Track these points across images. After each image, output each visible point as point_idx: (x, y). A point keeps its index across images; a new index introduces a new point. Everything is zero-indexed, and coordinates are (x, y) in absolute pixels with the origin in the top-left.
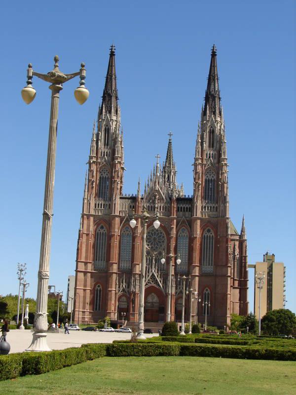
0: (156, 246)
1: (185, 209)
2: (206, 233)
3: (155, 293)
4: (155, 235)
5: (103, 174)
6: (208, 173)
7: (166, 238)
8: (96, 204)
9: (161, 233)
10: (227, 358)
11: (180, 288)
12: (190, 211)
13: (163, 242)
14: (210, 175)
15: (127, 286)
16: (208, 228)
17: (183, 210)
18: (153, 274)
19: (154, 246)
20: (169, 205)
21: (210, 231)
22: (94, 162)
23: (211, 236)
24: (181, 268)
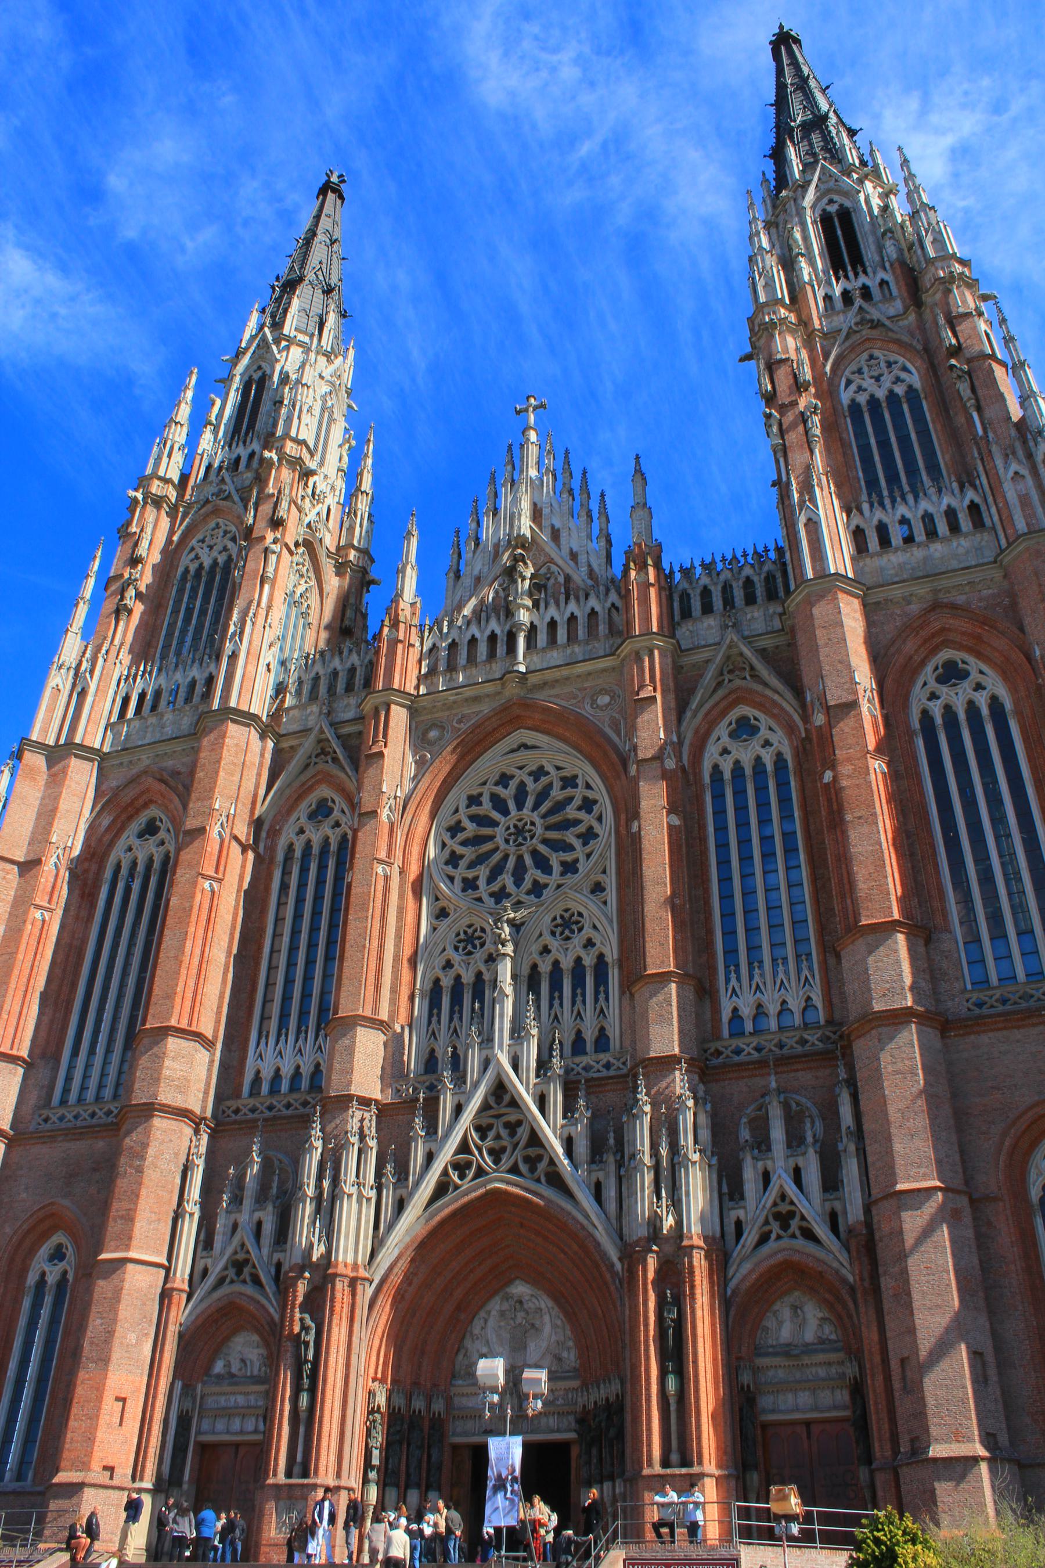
0: (533, 873)
1: (738, 594)
2: (933, 696)
3: (537, 1279)
4: (520, 806)
6: (860, 371)
8: (126, 700)
9: (569, 782)
11: (766, 1177)
14: (877, 379)
15: (268, 1228)
18: (500, 1089)
19: (518, 882)
20: (613, 597)
21: (964, 675)
22: (158, 502)
23: (982, 701)
24: (760, 1011)
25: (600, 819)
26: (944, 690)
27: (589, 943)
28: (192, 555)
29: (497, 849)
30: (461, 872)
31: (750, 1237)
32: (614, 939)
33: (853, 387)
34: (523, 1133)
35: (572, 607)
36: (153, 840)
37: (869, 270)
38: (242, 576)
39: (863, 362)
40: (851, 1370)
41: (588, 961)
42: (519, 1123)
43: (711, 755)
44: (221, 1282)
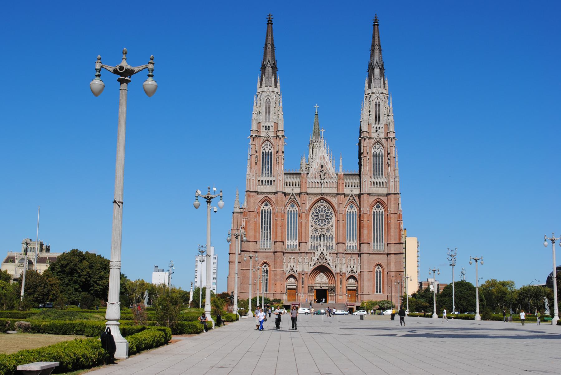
2: (375, 209)
4: (322, 212)
5: (266, 148)
7: (333, 214)
10: (433, 337)
12: (358, 187)
13: (331, 218)
14: (378, 149)
16: (378, 204)
17: (350, 186)
18: (322, 253)
19: (322, 223)
20: (336, 180)
25: (332, 216)
26: (377, 209)
27: (331, 234)
28: (263, 149)
29: (319, 218)
30: (314, 220)
31: (348, 272)
32: (334, 235)
33: (374, 150)
34: (325, 258)
35: (330, 180)
36: (268, 207)
37: (381, 124)
38: (278, 162)
39: (376, 145)
40: (357, 286)
41: (331, 236)
42: (324, 257)
43: (347, 209)
44: (289, 272)
